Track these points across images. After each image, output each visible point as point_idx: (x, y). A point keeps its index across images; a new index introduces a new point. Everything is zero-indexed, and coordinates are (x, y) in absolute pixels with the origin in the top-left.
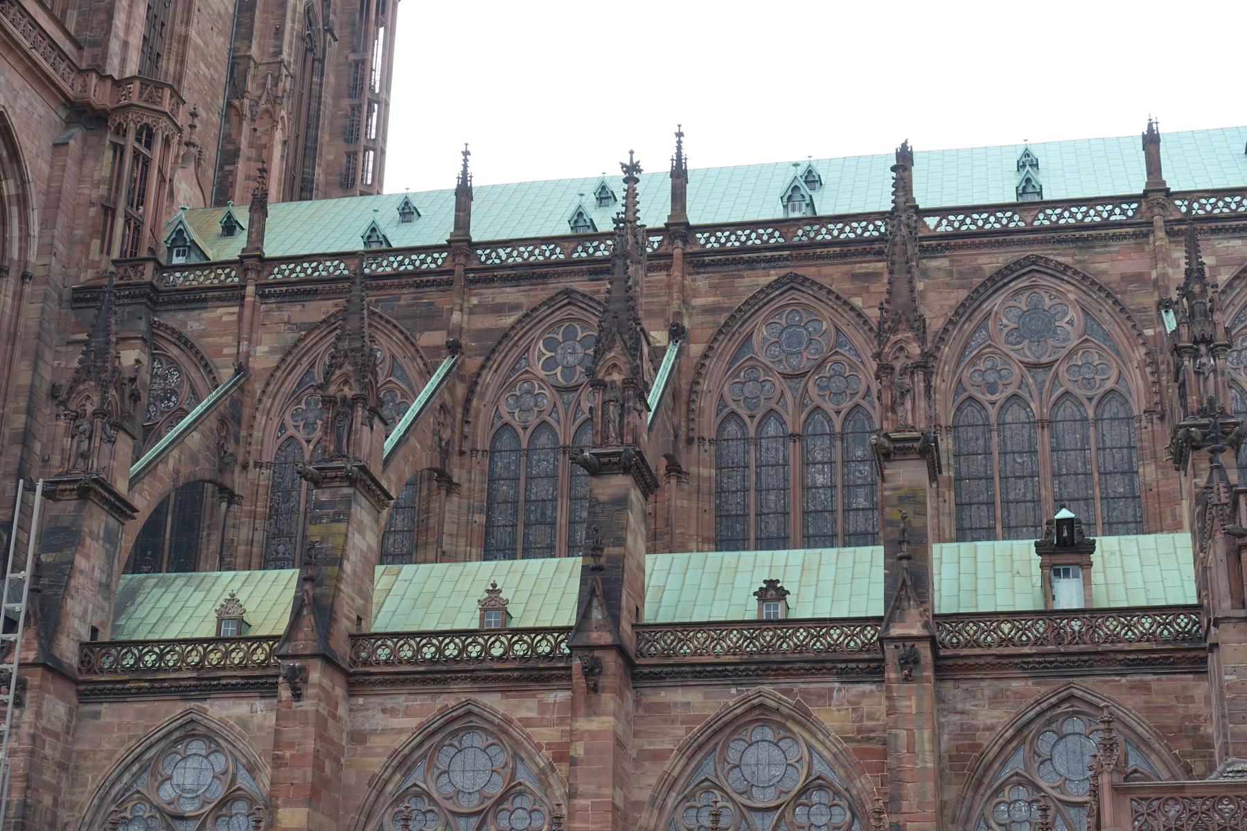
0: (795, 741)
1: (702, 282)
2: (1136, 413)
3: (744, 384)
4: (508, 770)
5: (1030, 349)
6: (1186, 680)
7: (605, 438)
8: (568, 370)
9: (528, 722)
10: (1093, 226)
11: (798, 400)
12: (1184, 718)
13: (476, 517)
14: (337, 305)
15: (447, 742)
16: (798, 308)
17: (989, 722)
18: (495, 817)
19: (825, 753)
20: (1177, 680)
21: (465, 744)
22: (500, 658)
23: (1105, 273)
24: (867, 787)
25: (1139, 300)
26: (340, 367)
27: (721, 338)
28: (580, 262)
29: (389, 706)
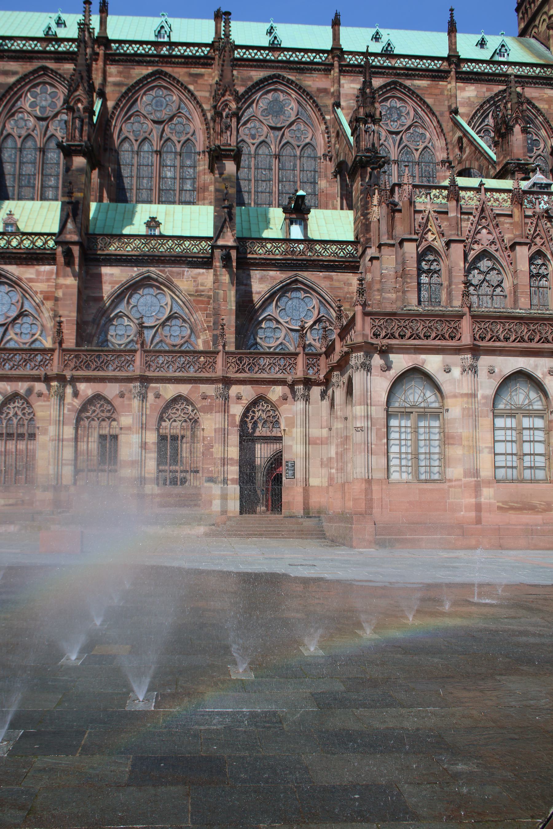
0: (165, 295)
1: (112, 69)
2: (319, 155)
3: (133, 123)
4: (20, 304)
8: (43, 108)
9: (30, 280)
10: (306, 63)
11: (159, 134)
12: (347, 293)
17: (258, 290)
18: (13, 327)
19: (179, 301)
23: (310, 86)
28: (50, 52)
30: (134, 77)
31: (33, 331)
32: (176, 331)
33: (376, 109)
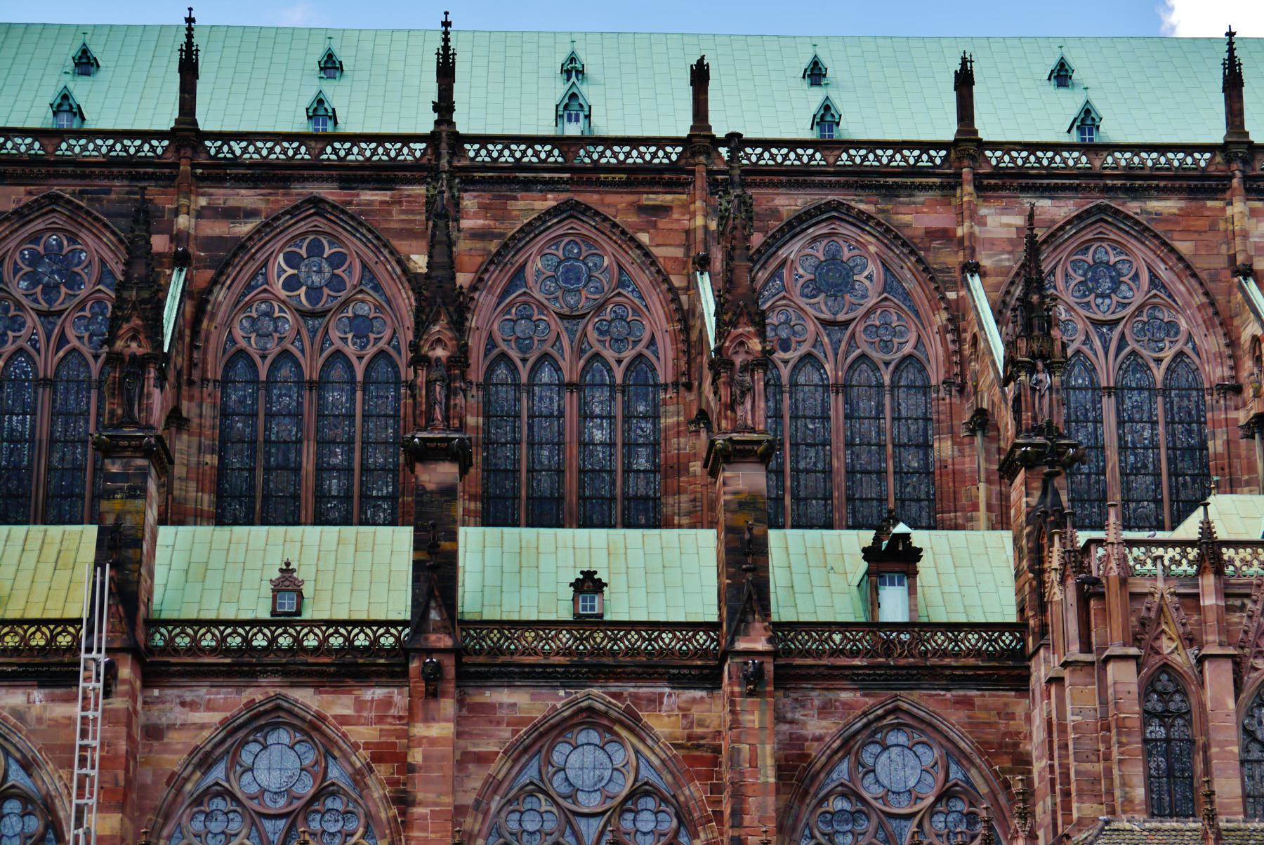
0: (623, 746)
1: (469, 201)
3: (515, 322)
5: (826, 304)
6: (1008, 697)
7: (430, 419)
8: (314, 293)
9: (344, 720)
11: (575, 344)
12: (1005, 734)
13: (208, 458)
14: (30, 193)
15: (251, 738)
16: (578, 240)
17: (818, 732)
18: (306, 819)
19: (653, 759)
20: (999, 696)
21: (270, 740)
22: (315, 651)
23: (908, 226)
24: (696, 795)
25: (942, 259)
26: (128, 320)
27: (492, 268)
28: (329, 166)
29: (188, 699)
30: (516, 218)
31: (351, 826)
32: (646, 822)
33: (1052, 340)
